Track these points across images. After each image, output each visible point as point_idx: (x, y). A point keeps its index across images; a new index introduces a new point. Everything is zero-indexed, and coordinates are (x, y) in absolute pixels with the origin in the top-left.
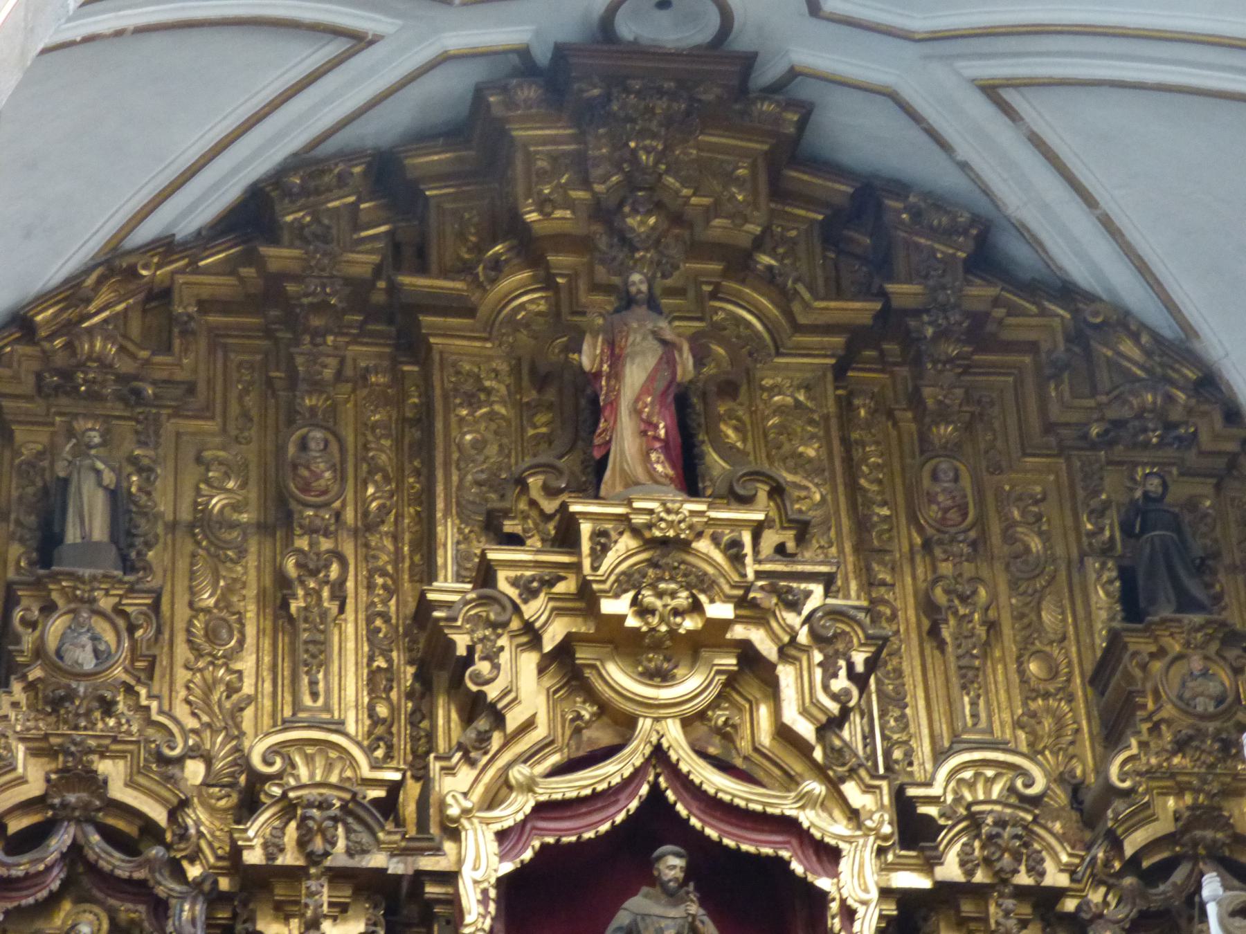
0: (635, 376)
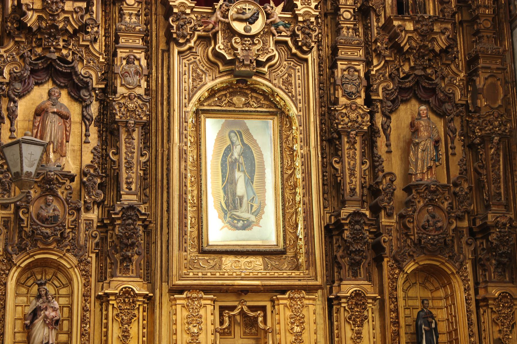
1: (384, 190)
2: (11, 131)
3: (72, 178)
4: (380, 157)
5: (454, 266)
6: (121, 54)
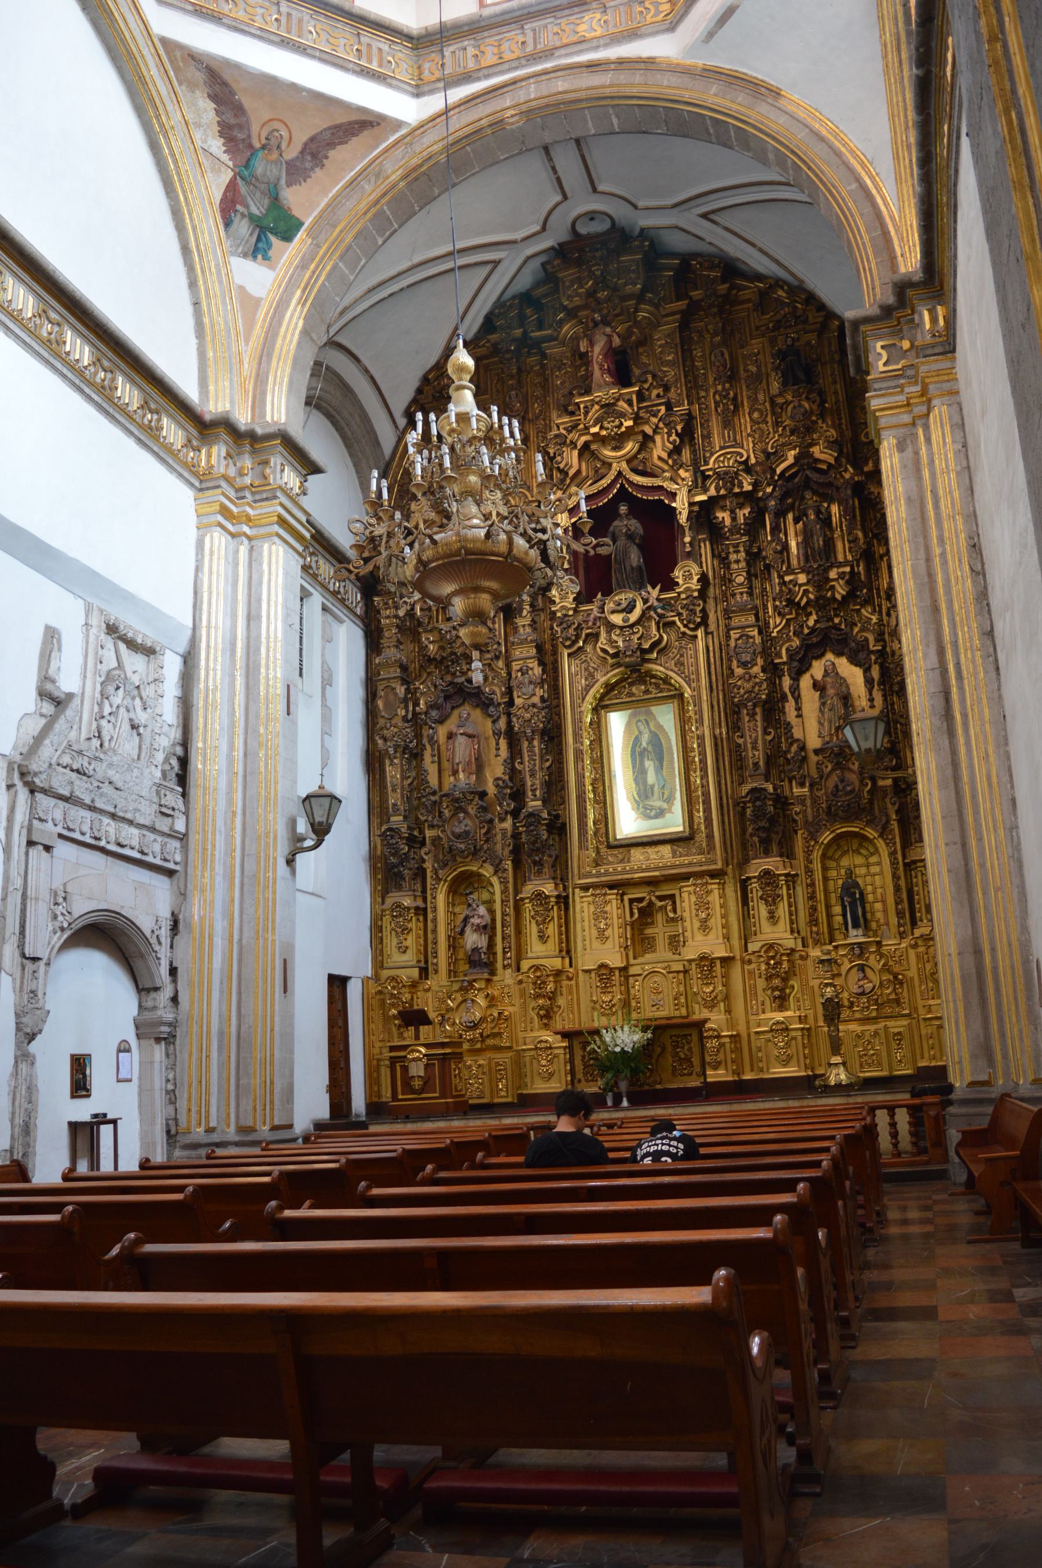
1: (793, 758)
2: (433, 756)
3: (483, 794)
4: (789, 723)
5: (874, 829)
6: (515, 666)
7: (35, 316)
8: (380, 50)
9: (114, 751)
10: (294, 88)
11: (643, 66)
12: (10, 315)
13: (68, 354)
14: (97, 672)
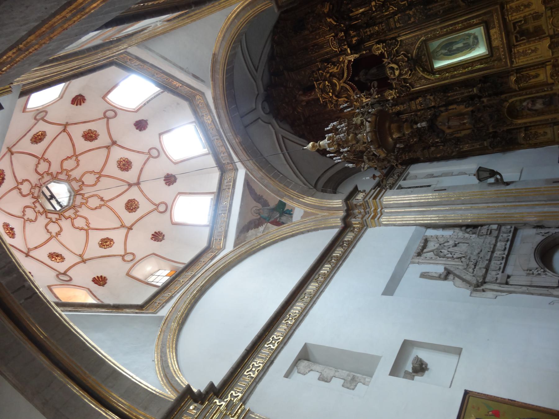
0: (305, 98)
2: (458, 133)
3: (473, 112)
6: (419, 108)
7: (317, 283)
8: (227, 182)
9: (466, 252)
10: (241, 207)
11: (216, 101)
12: (318, 290)
13: (328, 272)
14: (436, 259)
